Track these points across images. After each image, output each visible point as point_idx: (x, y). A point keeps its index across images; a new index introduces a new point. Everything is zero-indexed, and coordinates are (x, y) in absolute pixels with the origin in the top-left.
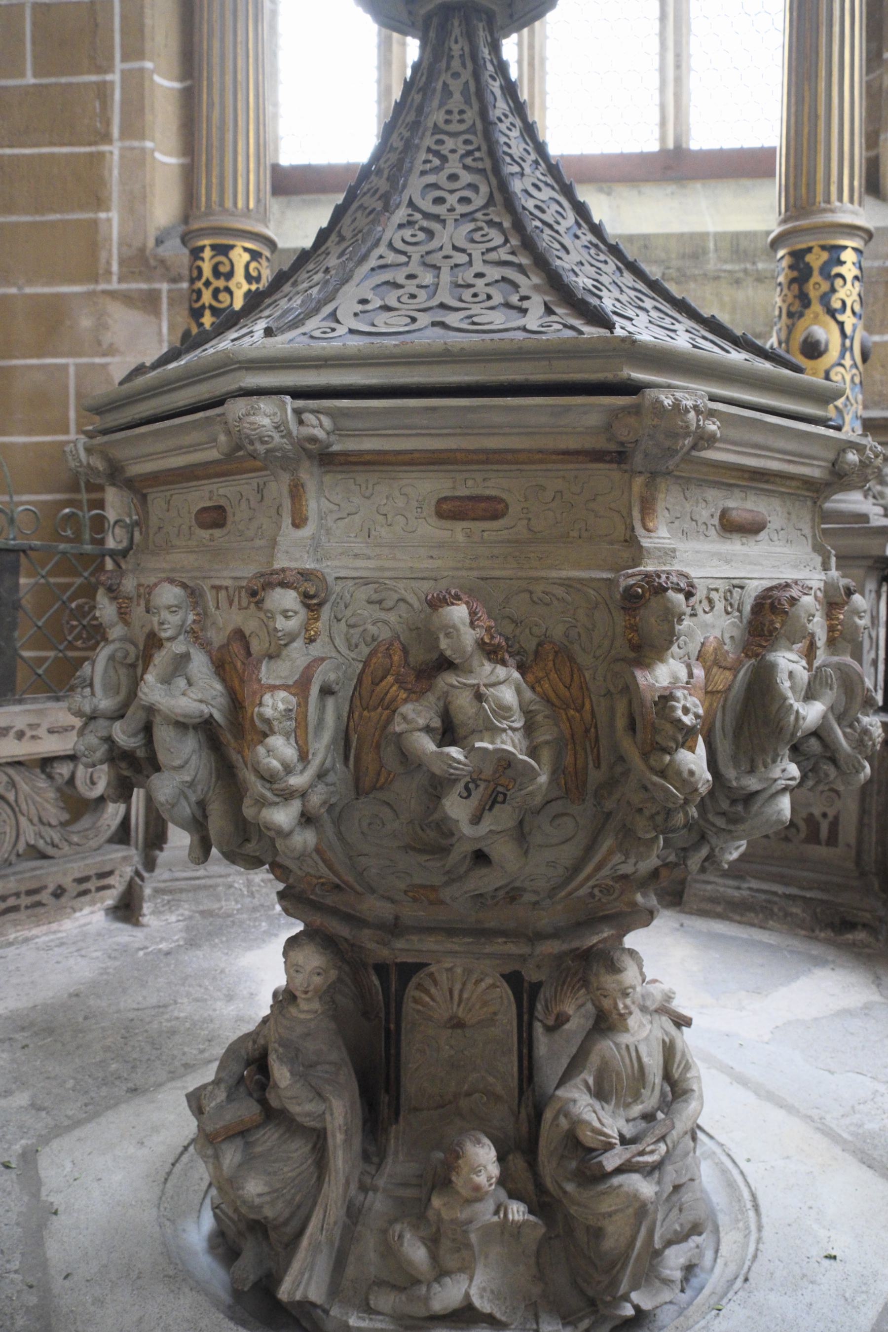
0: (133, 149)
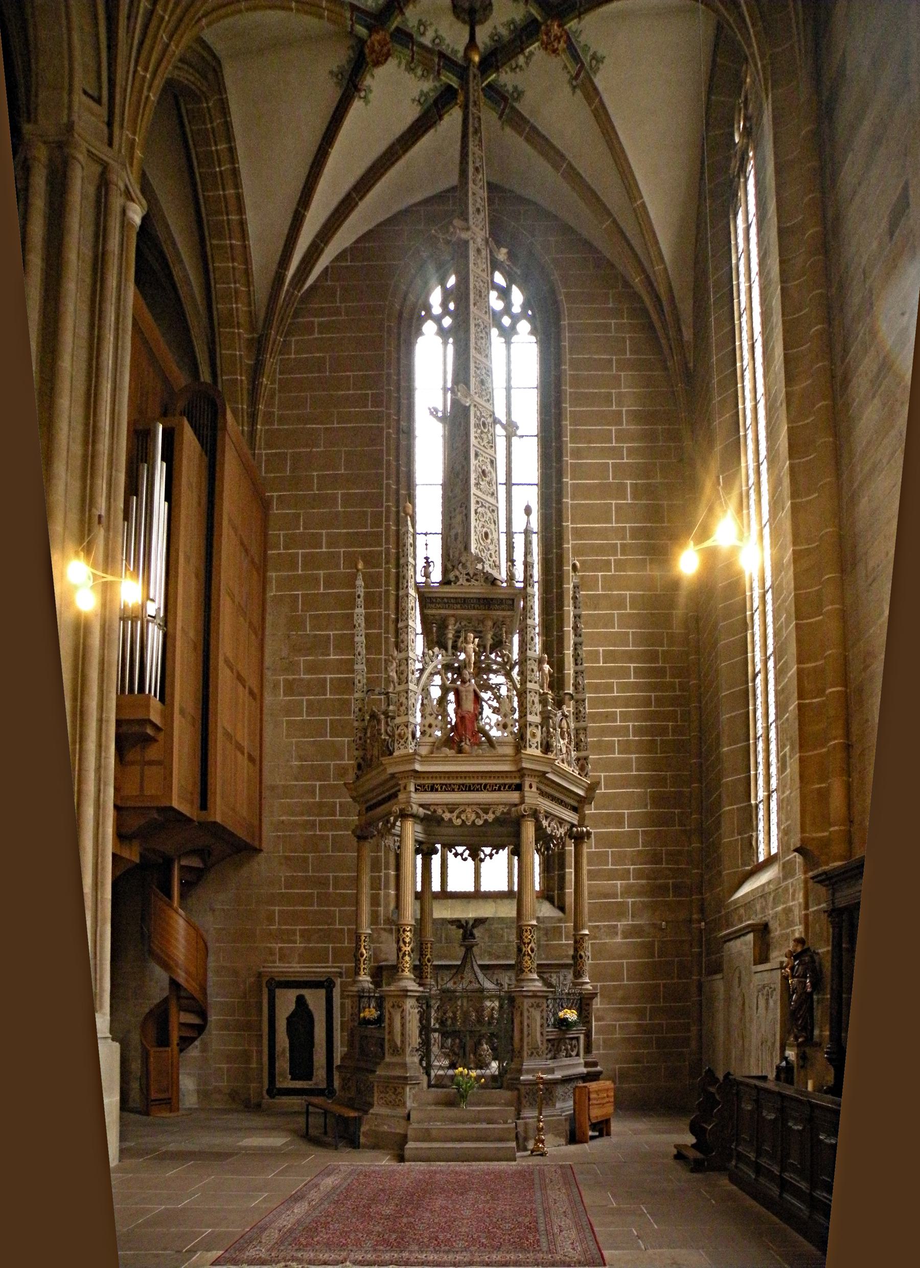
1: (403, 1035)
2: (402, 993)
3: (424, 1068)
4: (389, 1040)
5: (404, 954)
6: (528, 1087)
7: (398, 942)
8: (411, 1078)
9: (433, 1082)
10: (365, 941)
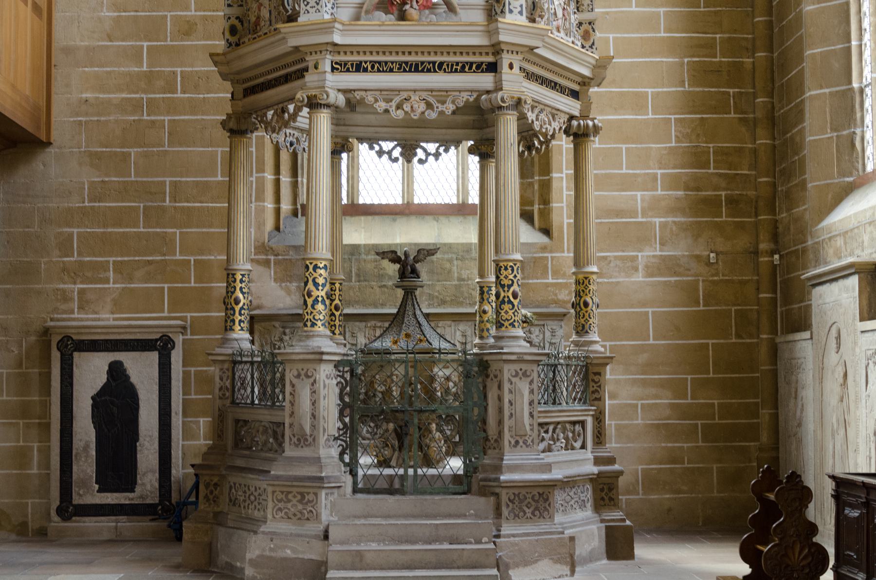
0: (259, 206)
1: (314, 416)
2: (317, 357)
3: (346, 465)
4: (291, 425)
5: (316, 301)
6: (511, 491)
7: (306, 284)
8: (327, 477)
9: (360, 486)
10: (241, 281)
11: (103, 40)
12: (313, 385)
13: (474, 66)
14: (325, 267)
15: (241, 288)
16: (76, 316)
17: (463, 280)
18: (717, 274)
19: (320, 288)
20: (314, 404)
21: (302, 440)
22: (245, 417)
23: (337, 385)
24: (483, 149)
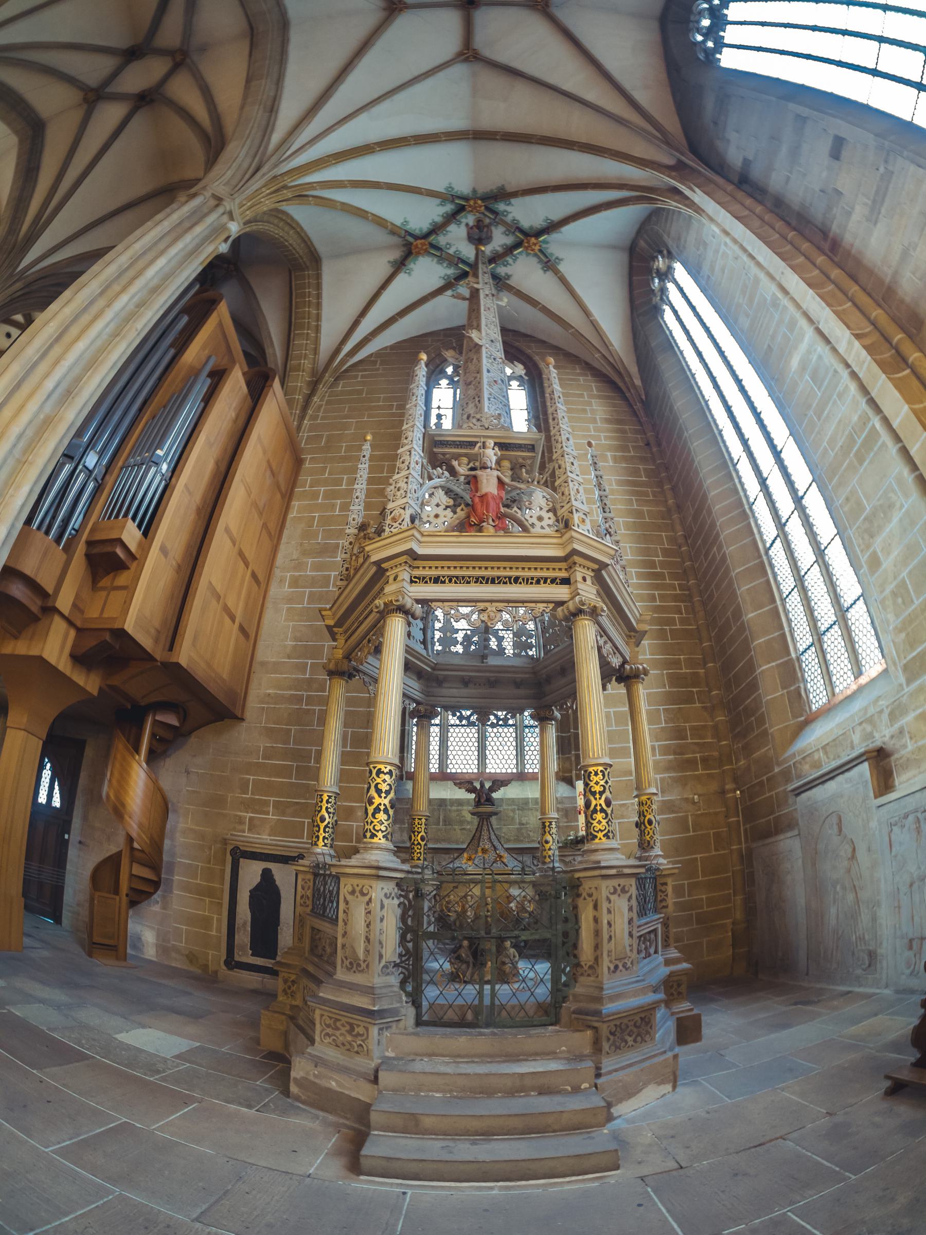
1: (368, 940)
4: (343, 946)
5: (377, 810)
11: (284, 658)
12: (368, 904)
13: (549, 581)
14: (390, 773)
15: (327, 808)
16: (246, 834)
17: (523, 824)
18: (699, 810)
19: (383, 795)
20: (368, 926)
21: (354, 965)
22: (317, 926)
23: (399, 905)
24: (542, 714)
